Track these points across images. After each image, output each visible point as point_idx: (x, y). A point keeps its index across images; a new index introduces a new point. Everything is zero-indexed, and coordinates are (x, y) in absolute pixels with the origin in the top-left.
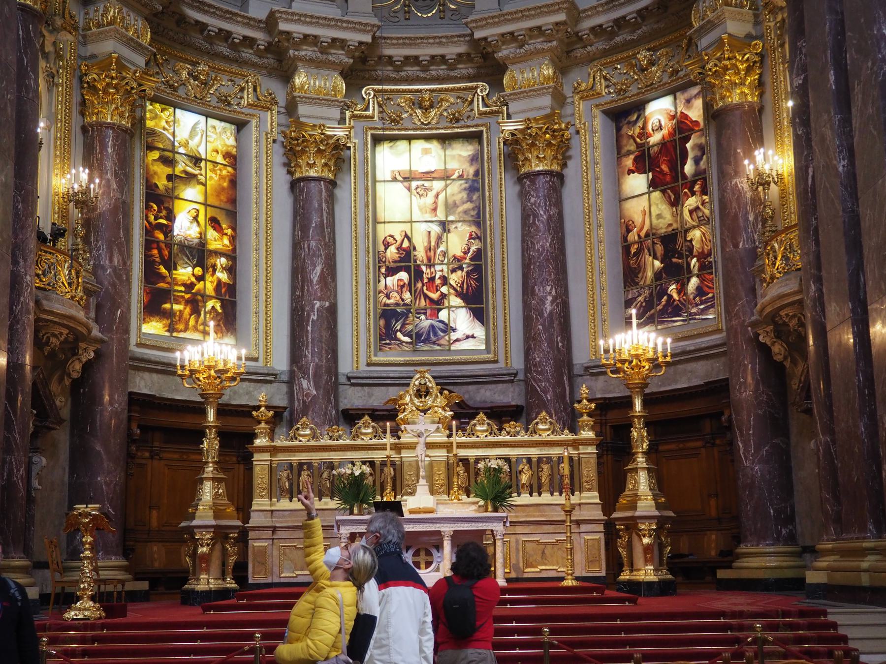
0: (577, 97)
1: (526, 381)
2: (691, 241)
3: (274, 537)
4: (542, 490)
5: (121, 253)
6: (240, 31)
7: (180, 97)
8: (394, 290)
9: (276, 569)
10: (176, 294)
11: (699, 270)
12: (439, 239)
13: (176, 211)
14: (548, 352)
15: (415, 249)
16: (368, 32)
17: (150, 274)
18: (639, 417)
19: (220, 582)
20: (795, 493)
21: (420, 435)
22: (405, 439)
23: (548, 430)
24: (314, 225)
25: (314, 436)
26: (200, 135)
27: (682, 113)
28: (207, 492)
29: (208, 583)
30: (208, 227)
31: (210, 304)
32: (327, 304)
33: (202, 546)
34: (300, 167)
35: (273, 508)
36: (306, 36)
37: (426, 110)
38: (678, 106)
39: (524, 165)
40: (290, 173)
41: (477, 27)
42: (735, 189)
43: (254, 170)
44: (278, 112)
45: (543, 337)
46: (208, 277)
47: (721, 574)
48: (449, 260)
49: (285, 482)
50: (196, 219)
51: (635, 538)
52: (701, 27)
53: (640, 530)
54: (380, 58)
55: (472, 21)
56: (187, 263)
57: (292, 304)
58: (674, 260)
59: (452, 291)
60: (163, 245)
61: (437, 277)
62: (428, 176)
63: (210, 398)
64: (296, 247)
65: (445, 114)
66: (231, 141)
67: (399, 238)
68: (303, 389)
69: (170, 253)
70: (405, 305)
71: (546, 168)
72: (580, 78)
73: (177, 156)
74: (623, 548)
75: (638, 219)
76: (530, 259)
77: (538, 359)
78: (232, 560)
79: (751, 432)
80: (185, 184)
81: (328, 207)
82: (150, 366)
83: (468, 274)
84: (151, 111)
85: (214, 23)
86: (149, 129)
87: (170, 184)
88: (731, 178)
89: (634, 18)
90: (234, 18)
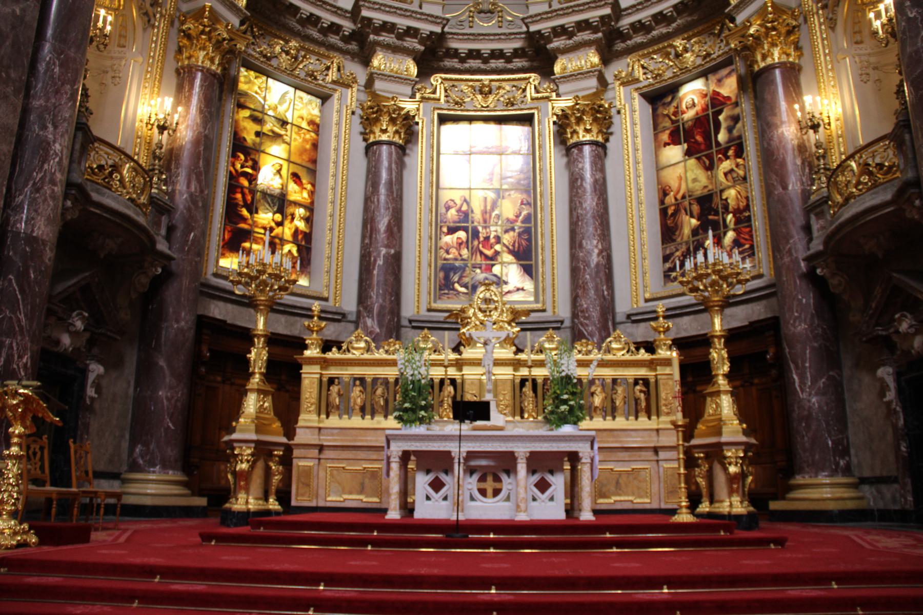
0: (618, 82)
2: (726, 199)
3: (321, 456)
4: (616, 414)
5: (199, 181)
6: (328, 18)
7: (272, 66)
8: (453, 247)
9: (321, 492)
11: (736, 224)
12: (494, 205)
13: (261, 163)
14: (595, 299)
15: (472, 211)
16: (438, 23)
17: (232, 213)
18: (719, 337)
19: (261, 502)
20: (849, 425)
21: (488, 342)
22: (468, 353)
23: (623, 349)
24: (383, 182)
25: (368, 350)
27: (714, 91)
28: (251, 403)
29: (247, 503)
31: (287, 248)
32: (393, 251)
33: (242, 462)
34: (374, 133)
35: (321, 425)
36: (385, 23)
37: (486, 94)
39: (572, 137)
40: (365, 140)
41: (533, 22)
42: (782, 137)
43: (333, 135)
44: (358, 90)
46: (287, 223)
47: (774, 505)
48: (503, 222)
49: (335, 398)
50: (279, 172)
51: (718, 469)
53: (725, 458)
54: (448, 49)
55: (526, 18)
56: (267, 209)
58: (710, 217)
59: (505, 249)
60: (247, 191)
61: (492, 236)
63: (261, 305)
64: (368, 200)
65: (502, 99)
66: (316, 112)
67: (459, 202)
68: (367, 327)
69: (253, 198)
70: (463, 260)
71: (592, 138)
72: (619, 67)
73: (266, 117)
74: (702, 478)
75: (674, 184)
76: (578, 217)
77: (585, 306)
78: (276, 479)
79: (807, 365)
80: (271, 141)
81: (397, 168)
82: (225, 295)
83: (520, 234)
84: (245, 76)
86: (242, 91)
87: (258, 140)
88: (777, 127)
89: (671, 12)
90: (324, 6)
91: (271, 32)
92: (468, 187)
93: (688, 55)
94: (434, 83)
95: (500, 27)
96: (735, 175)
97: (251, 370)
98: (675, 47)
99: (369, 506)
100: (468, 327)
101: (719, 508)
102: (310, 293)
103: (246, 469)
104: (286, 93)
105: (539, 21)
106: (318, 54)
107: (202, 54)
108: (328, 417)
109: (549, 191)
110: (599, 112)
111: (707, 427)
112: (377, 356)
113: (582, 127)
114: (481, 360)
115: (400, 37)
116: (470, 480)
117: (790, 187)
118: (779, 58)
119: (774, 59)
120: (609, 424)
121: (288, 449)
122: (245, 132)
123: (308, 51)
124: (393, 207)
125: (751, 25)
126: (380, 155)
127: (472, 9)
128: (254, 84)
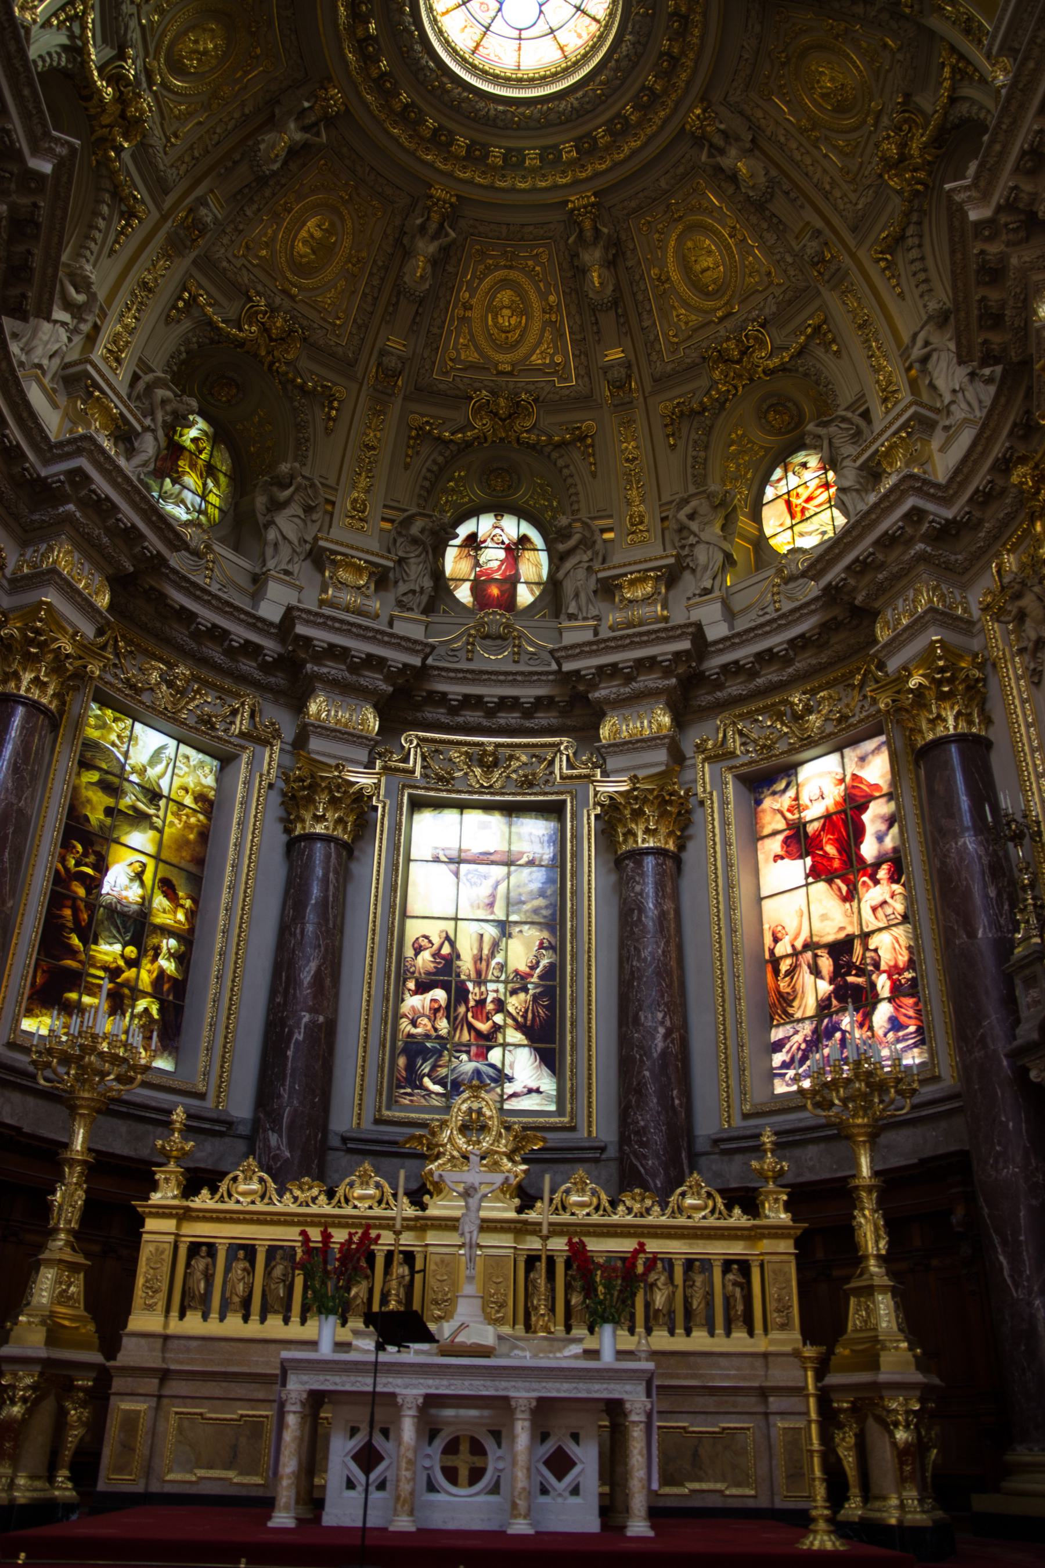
1: (622, 1160)
2: (876, 950)
6: (241, 633)
8: (424, 1015)
10: (90, 979)
12: (495, 946)
13: (110, 859)
15: (458, 957)
16: (417, 652)
18: (870, 1189)
21: (471, 1191)
22: (438, 1208)
23: (705, 1207)
26: (164, 763)
27: (854, 775)
30: (156, 890)
31: (141, 1005)
32: (321, 1019)
34: (303, 821)
36: (332, 646)
37: (488, 767)
38: (847, 767)
39: (625, 841)
40: (287, 831)
41: (568, 658)
44: (281, 750)
45: (651, 1088)
46: (146, 964)
48: (507, 977)
49: (199, 1281)
50: (139, 876)
52: (893, 640)
54: (431, 693)
55: (558, 650)
56: (115, 937)
57: (268, 1015)
59: (509, 1021)
60: (82, 905)
61: (489, 999)
62: (485, 859)
63: (82, 1107)
65: (514, 776)
66: (210, 781)
67: (436, 941)
68: (269, 1147)
69: (91, 917)
70: (439, 1037)
73: (126, 784)
76: (632, 973)
78: (74, 1435)
79: (1022, 1238)
81: (337, 880)
82: (25, 1083)
83: (535, 998)
84: (97, 717)
85: (208, 616)
86: (90, 740)
87: (108, 821)
91: (146, 650)
92: (452, 914)
93: (812, 717)
94: (406, 746)
95: (515, 662)
96: (889, 911)
97: (52, 1223)
98: (792, 704)
99: (244, 1492)
100: (440, 1161)
101: (879, 1510)
102: (175, 1085)
103: (19, 1416)
104: (164, 747)
105: (577, 655)
106: (221, 689)
107: (27, 677)
108: (182, 1316)
109: (586, 928)
110: (670, 803)
111: (852, 1351)
112: (279, 1207)
113: (642, 827)
114: (457, 1219)
115: (354, 669)
116: (429, 1450)
117: (980, 934)
118: (955, 728)
119: (948, 729)
120: (680, 1343)
121: (104, 1377)
122: (89, 807)
123: (205, 683)
124: (327, 945)
125: (910, 675)
126: (310, 857)
127: (473, 632)
128: (111, 729)
